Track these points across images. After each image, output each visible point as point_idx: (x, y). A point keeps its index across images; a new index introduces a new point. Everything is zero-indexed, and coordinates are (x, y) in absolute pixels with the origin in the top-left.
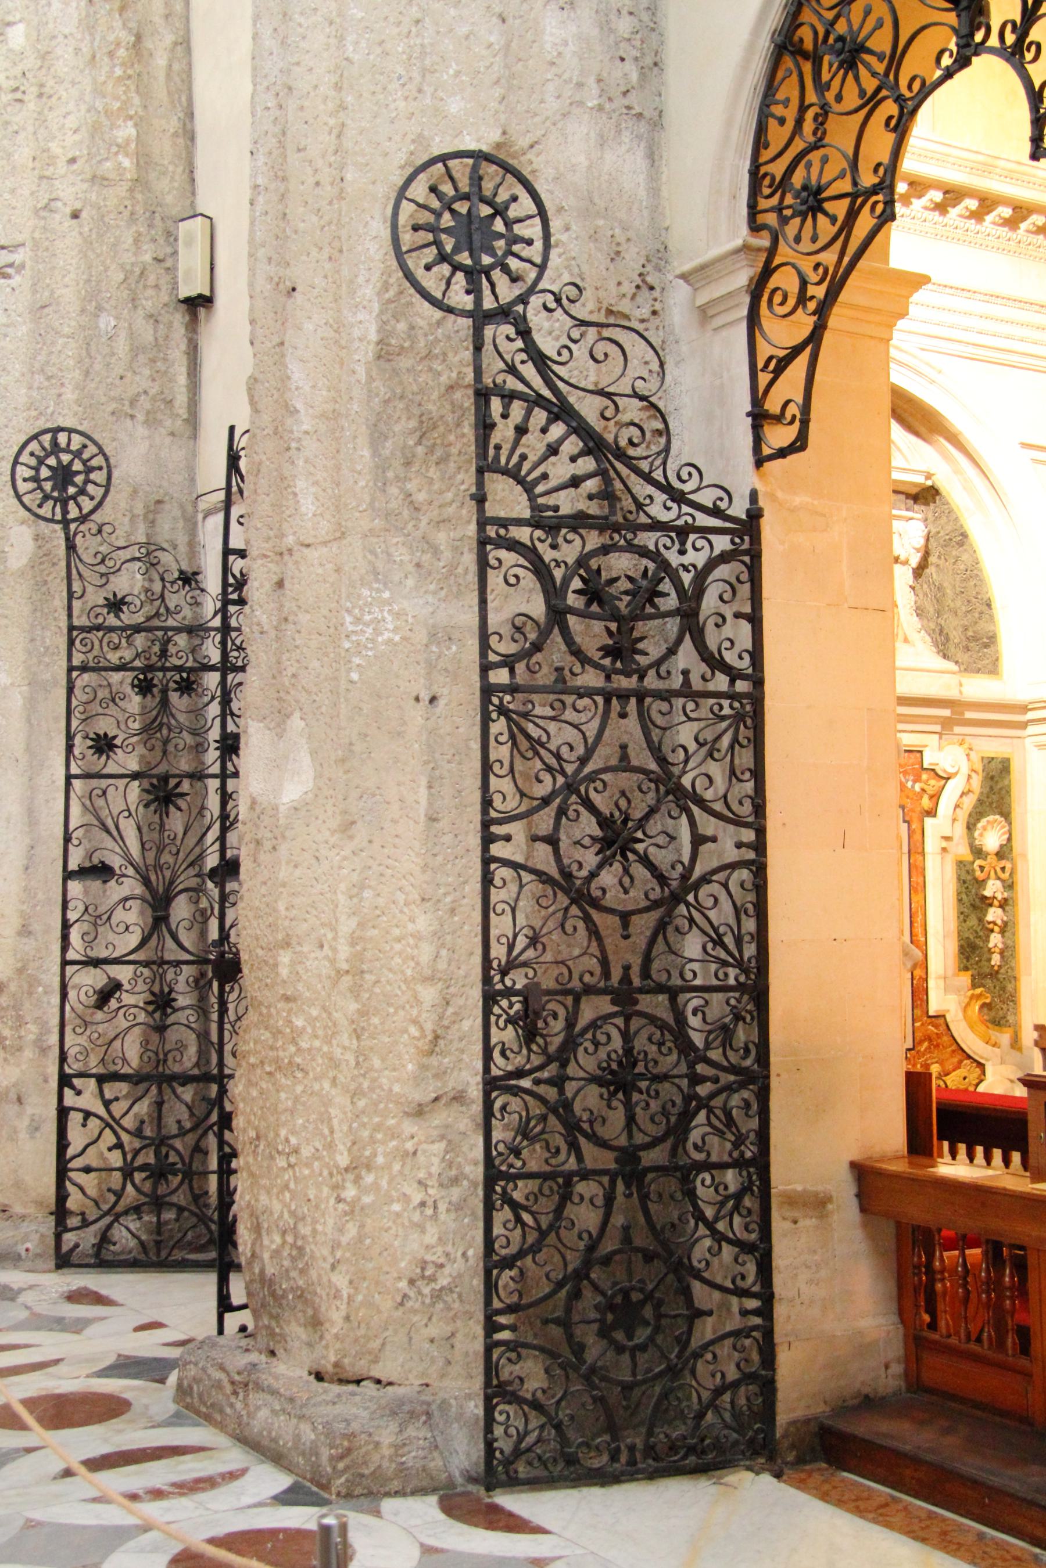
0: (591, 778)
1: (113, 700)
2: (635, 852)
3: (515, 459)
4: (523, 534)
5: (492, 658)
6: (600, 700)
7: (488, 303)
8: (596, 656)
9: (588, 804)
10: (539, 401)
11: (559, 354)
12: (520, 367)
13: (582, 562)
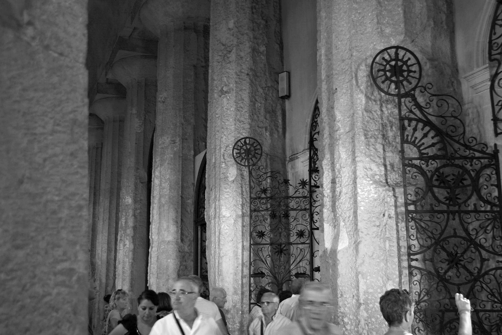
0: (444, 240)
1: (264, 220)
2: (460, 264)
3: (413, 139)
4: (417, 162)
5: (409, 202)
6: (446, 214)
7: (402, 91)
8: (444, 200)
9: (443, 248)
10: (419, 120)
11: (426, 106)
12: (413, 110)
13: (437, 170)
